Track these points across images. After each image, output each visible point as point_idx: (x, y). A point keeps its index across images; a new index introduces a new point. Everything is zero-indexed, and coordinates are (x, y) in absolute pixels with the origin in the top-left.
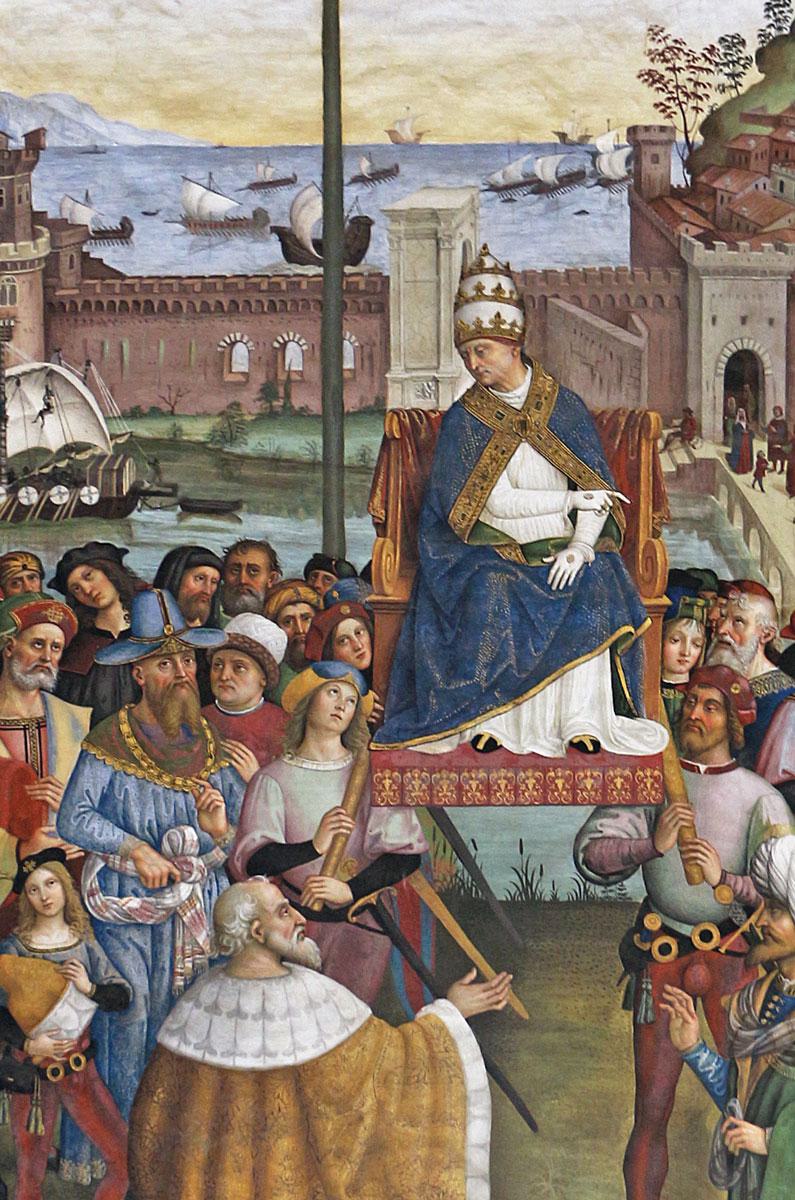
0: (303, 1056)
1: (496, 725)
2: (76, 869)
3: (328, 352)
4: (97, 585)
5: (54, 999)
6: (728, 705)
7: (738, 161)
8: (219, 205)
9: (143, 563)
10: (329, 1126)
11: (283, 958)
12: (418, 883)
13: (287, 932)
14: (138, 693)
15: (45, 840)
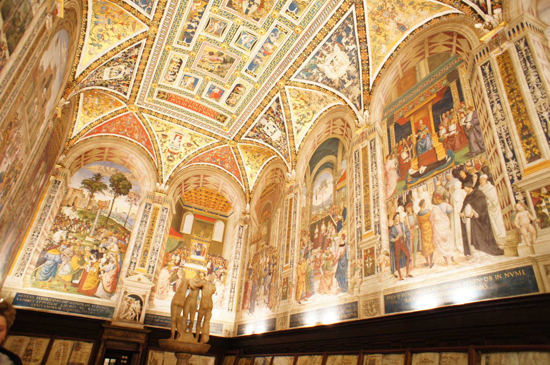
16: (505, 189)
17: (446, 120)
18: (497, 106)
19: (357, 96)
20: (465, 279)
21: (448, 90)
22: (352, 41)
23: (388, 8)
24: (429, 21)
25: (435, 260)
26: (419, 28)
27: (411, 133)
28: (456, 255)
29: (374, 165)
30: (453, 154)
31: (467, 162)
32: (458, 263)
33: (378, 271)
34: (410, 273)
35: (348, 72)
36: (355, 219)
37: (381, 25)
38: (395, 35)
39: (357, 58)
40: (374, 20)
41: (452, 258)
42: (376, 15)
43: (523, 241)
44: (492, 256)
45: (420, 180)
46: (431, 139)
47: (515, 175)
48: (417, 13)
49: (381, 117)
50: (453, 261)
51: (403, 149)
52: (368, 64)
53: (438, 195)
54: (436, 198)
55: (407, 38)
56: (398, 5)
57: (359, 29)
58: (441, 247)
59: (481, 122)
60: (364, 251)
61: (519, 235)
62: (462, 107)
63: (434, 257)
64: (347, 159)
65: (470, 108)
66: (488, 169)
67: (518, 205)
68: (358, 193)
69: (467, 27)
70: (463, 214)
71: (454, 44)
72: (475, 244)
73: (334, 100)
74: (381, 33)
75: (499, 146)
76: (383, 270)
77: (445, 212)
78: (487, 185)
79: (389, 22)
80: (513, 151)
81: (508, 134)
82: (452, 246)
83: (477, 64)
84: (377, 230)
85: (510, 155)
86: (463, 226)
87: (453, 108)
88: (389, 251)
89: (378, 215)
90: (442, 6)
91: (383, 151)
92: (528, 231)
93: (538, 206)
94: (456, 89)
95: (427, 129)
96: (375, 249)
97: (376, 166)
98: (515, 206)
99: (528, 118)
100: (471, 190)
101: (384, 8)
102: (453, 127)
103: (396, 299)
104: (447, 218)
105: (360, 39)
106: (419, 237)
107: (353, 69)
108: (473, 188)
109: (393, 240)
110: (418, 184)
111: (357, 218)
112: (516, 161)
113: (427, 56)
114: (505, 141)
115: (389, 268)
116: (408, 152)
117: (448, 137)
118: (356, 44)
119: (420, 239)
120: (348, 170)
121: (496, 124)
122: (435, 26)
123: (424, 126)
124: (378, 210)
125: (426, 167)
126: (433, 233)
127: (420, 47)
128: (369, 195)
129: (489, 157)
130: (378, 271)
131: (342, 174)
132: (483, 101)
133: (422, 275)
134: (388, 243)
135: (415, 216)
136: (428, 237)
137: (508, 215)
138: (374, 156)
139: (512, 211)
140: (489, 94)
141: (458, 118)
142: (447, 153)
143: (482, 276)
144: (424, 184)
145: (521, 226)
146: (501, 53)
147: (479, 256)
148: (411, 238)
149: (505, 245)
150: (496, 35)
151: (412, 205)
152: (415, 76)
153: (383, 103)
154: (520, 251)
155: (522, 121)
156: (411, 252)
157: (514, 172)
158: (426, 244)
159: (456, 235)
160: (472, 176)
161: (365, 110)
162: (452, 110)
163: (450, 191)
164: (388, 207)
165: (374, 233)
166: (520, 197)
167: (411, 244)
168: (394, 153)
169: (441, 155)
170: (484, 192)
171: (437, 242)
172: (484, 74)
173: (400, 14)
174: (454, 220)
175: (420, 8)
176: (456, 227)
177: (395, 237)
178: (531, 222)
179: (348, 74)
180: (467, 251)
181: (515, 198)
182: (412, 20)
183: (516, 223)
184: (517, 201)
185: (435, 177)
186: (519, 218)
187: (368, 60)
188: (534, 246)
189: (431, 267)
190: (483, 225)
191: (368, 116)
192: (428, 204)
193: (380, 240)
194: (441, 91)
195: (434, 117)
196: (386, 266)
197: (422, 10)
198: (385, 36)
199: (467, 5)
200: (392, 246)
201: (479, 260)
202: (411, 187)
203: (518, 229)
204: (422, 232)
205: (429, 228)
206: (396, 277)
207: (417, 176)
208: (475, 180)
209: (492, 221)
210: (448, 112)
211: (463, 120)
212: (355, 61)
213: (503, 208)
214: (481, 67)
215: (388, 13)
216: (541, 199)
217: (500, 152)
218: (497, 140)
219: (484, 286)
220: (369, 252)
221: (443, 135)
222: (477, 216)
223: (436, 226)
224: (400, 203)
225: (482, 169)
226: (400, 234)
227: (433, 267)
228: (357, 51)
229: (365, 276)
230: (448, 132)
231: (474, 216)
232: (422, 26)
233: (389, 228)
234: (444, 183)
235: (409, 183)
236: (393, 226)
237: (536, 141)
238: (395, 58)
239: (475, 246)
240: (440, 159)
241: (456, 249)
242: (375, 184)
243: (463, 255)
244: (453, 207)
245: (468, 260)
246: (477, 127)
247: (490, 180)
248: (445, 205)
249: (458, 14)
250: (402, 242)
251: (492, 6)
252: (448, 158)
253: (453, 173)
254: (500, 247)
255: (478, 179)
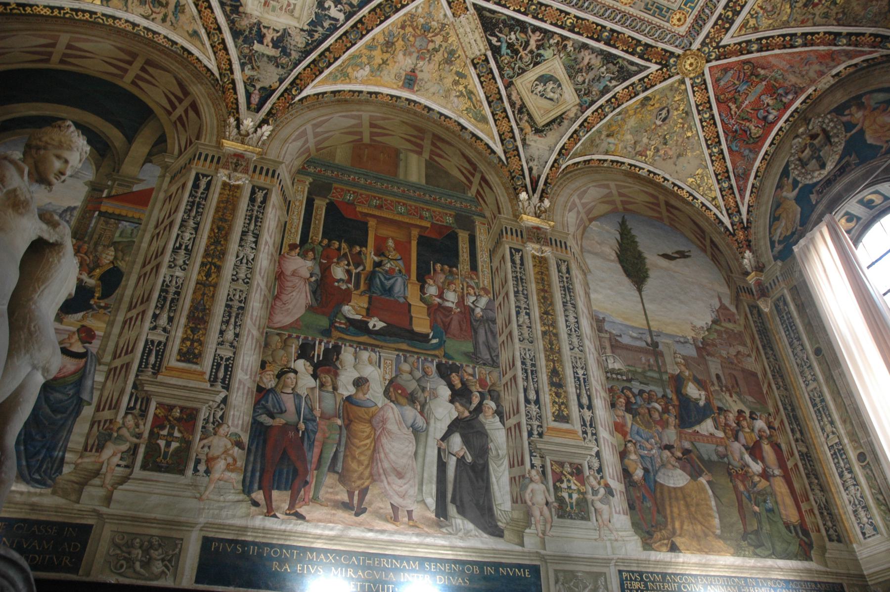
0: (681, 485)
1: (697, 428)
2: (635, 444)
3: (657, 361)
4: (628, 393)
5: (636, 469)
6: (732, 430)
7: (708, 345)
8: (635, 335)
9: (636, 391)
10: (688, 499)
11: (673, 466)
12: (692, 454)
13: (673, 461)
14: (639, 414)
15: (629, 438)
16: (518, 439)
17: (441, 278)
18: (523, 318)
19: (267, 86)
20: (430, 560)
21: (454, 237)
22: (348, 8)
23: (432, 41)
24: (446, 117)
25: (370, 504)
26: (426, 107)
27: (364, 244)
28: (418, 511)
29: (250, 238)
30: (444, 338)
31: (467, 366)
32: (421, 526)
33: (196, 470)
34: (302, 510)
35: (285, 33)
36: (150, 313)
37: (400, 44)
38: (393, 77)
39: (325, 38)
40: (403, 27)
41: (410, 513)
42: (411, 26)
43: (533, 527)
44: (485, 535)
45: (364, 339)
46: (405, 285)
47: (535, 427)
48: (449, 91)
49: (298, 163)
50: (410, 518)
51: (339, 259)
52: (330, 64)
53: (398, 387)
54: (396, 390)
55: (398, 98)
56: (446, 55)
57: (378, 10)
58: (389, 483)
59: (500, 322)
60: (160, 405)
61: (529, 514)
62: (472, 279)
63: (368, 497)
64: (166, 168)
65: (487, 292)
66: (499, 395)
67: (534, 472)
68: (180, 262)
69: (497, 179)
70: (444, 445)
71: (476, 180)
72: (458, 504)
73: (195, 34)
74: (387, 52)
75: (520, 375)
76: (216, 475)
77: (410, 422)
78: (493, 420)
79: (410, 54)
80: (537, 392)
81: (533, 365)
82: (413, 491)
83: (504, 239)
84: (221, 374)
85: (532, 396)
86: (442, 466)
87: (457, 268)
88: (245, 438)
89: (232, 345)
90: (487, 123)
91: (284, 228)
92: (541, 515)
93: (558, 484)
94: (467, 245)
95: (401, 263)
96: (202, 416)
97: (256, 243)
98: (529, 473)
99: (560, 361)
100: (467, 414)
101: (430, 35)
102: (451, 297)
103: (244, 556)
104: (412, 436)
105: (360, 21)
106: (339, 444)
107: (299, 40)
108: (470, 412)
109: (265, 419)
110: (360, 343)
111: (155, 317)
112: (539, 408)
113: (426, 155)
114: (529, 372)
115: (236, 478)
116: (349, 272)
117: (439, 304)
118: (347, 19)
119: (342, 449)
120: (162, 196)
121: (520, 340)
122: (447, 129)
123: (393, 254)
124: (237, 335)
125: (384, 325)
126: (374, 450)
127: (415, 133)
128: (215, 286)
129: (504, 381)
130: (196, 470)
131: (136, 188)
132: (507, 294)
133: (331, 522)
134: (248, 419)
135: (339, 400)
136: (361, 453)
137: (517, 479)
138: (256, 218)
139: (524, 476)
140: (516, 293)
141: (463, 289)
142: (432, 328)
143: (463, 563)
144: (373, 350)
145: (533, 504)
146: (539, 254)
147: (461, 527)
148: (319, 436)
149: (507, 524)
150: (538, 228)
151: (336, 375)
152: (397, 166)
153: (311, 144)
154: (526, 540)
155: (553, 361)
156: (314, 466)
157: (536, 423)
158: (354, 465)
159: (425, 475)
160: (471, 392)
161: (265, 122)
162: (454, 269)
163: (426, 394)
164: (267, 345)
165: (207, 377)
166: (537, 462)
167: (316, 450)
168: (313, 250)
169: (421, 324)
170: (487, 427)
171: (381, 471)
172: (513, 262)
173: (433, 66)
174: (425, 447)
175: (461, 92)
176: (427, 460)
177: (272, 416)
178: (547, 503)
179: (283, 36)
180: (441, 511)
181: (531, 460)
182: (432, 90)
183: (527, 497)
184: (533, 466)
185: (401, 354)
186: (532, 491)
187: (336, 59)
188: (546, 537)
189: (357, 515)
190: (477, 481)
191: (265, 138)
192: (376, 393)
193: (225, 401)
194: (441, 227)
195: (418, 255)
196: (229, 468)
197: (458, 97)
198: (384, 62)
199: (520, 160)
200: (258, 431)
201: (460, 534)
202: (340, 339)
203: (529, 507)
204: (348, 438)
205: (368, 437)
206: (255, 504)
207: (360, 327)
208: (476, 401)
209: (493, 479)
210: (446, 267)
211: (473, 299)
212: (316, 36)
213: (512, 466)
214: (511, 248)
215: (424, 45)
216: (564, 478)
217: (521, 384)
218: (519, 364)
219: (463, 580)
220: (177, 413)
221: (431, 296)
222: (469, 459)
223: (384, 440)
224: (305, 352)
225: (489, 391)
226: (290, 416)
227: (363, 516)
228: (336, 29)
229: (144, 467)
230: (441, 296)
231: (463, 457)
232: (430, 109)
233: (260, 389)
234: (418, 374)
235: (337, 328)
236: (272, 390)
237: (566, 397)
238: (360, 102)
239: (457, 507)
240: (417, 329)
241: (420, 498)
242: (242, 275)
243: (433, 516)
244: (428, 423)
245: (441, 527)
246: (491, 325)
247: (499, 413)
248: (411, 413)
249: (493, 152)
250: (291, 434)
251: (543, 191)
252: (434, 337)
253: (439, 366)
254: (499, 524)
255: (480, 403)
